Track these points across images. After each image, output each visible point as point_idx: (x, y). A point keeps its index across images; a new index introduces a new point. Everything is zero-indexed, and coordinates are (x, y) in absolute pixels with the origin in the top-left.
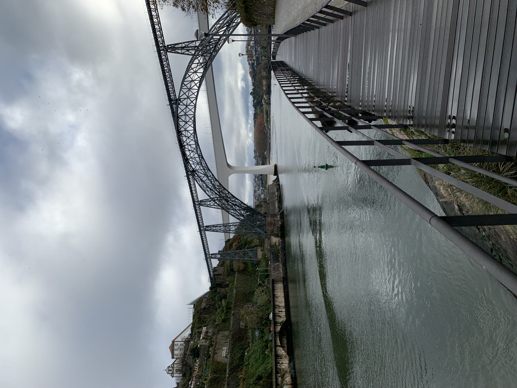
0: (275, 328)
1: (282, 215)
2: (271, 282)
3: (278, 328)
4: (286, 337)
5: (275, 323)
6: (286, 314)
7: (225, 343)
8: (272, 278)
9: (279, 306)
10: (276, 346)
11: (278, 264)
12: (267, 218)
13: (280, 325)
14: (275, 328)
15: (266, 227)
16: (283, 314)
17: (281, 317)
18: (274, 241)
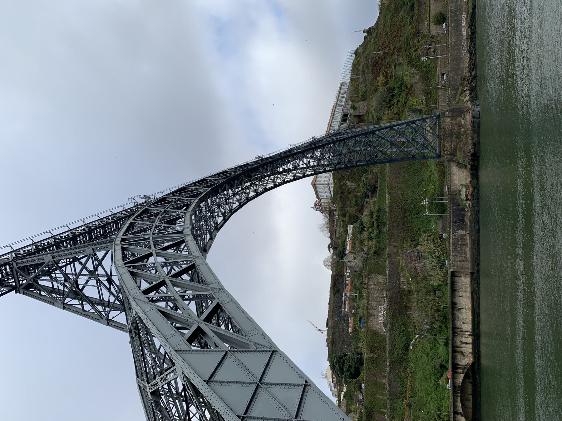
0: (454, 378)
1: (476, 125)
2: (450, 274)
3: (460, 379)
4: (471, 380)
5: (455, 367)
6: (473, 350)
7: (381, 297)
8: (452, 270)
9: (462, 331)
10: (455, 413)
11: (463, 233)
12: (442, 119)
13: (462, 373)
14: (454, 378)
15: (440, 143)
16: (468, 349)
17: (464, 355)
18: (456, 182)
